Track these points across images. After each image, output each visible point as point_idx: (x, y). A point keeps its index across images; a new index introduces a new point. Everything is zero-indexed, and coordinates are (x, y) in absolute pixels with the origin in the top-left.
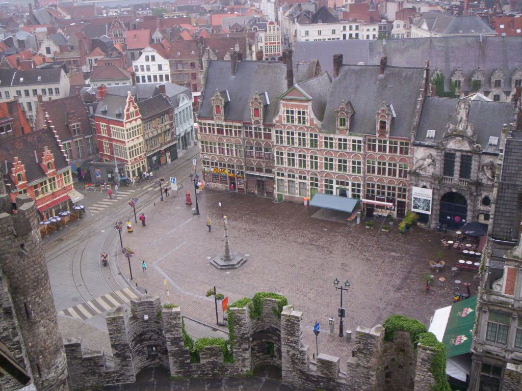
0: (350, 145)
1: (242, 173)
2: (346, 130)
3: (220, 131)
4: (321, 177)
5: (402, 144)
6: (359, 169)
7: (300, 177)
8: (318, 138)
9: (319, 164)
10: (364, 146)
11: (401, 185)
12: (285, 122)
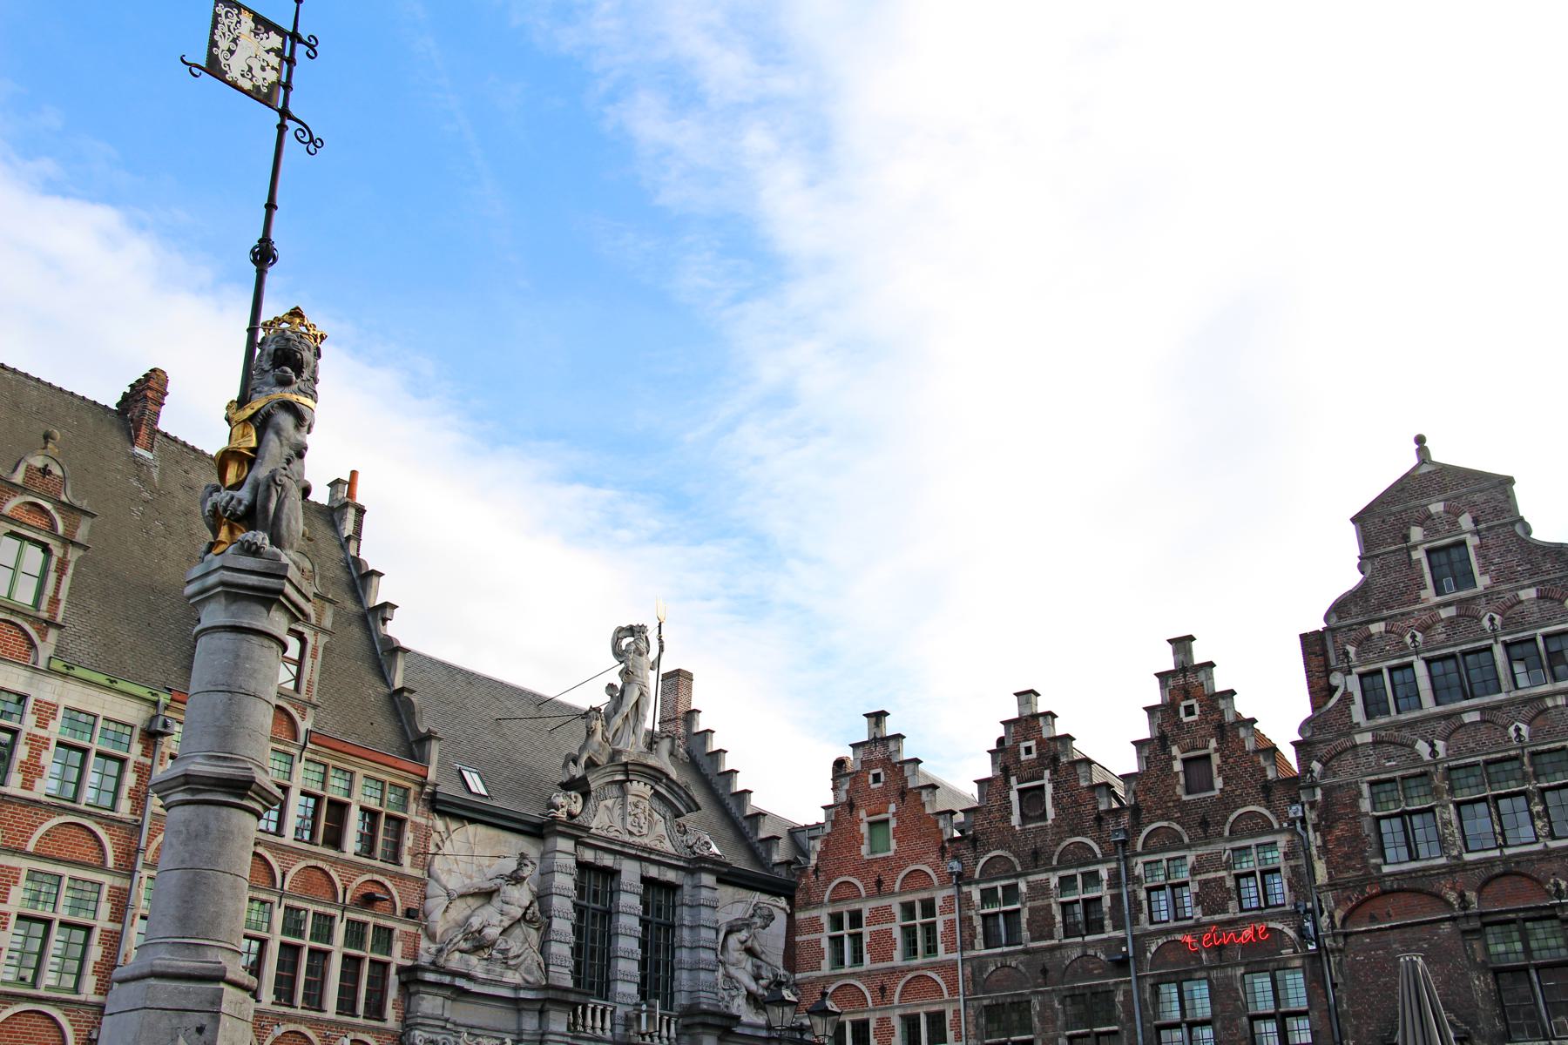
0: (38, 744)
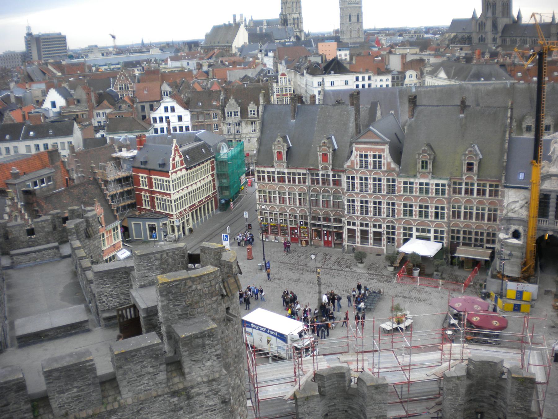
1: (306, 224)
2: (429, 173)
3: (282, 180)
4: (399, 224)
5: (491, 186)
6: (443, 214)
7: (374, 226)
8: (396, 183)
9: (396, 211)
10: (449, 190)
11: (491, 230)
12: (357, 167)
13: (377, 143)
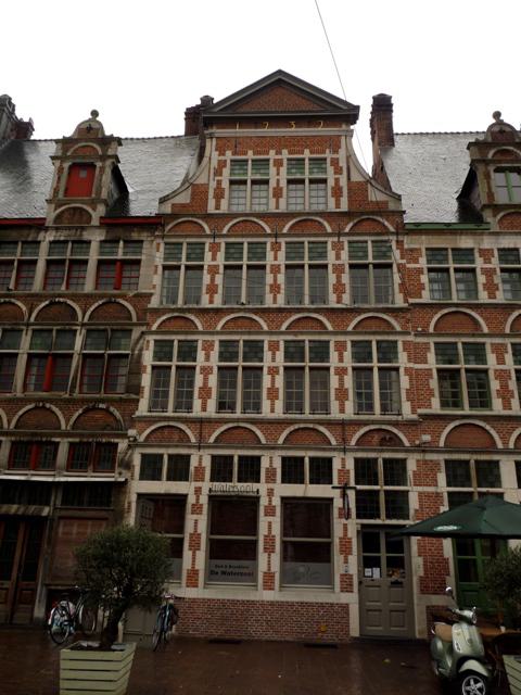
7: (292, 470)
9: (405, 382)
13: (310, 120)
